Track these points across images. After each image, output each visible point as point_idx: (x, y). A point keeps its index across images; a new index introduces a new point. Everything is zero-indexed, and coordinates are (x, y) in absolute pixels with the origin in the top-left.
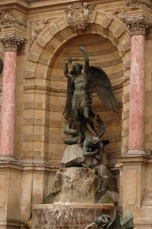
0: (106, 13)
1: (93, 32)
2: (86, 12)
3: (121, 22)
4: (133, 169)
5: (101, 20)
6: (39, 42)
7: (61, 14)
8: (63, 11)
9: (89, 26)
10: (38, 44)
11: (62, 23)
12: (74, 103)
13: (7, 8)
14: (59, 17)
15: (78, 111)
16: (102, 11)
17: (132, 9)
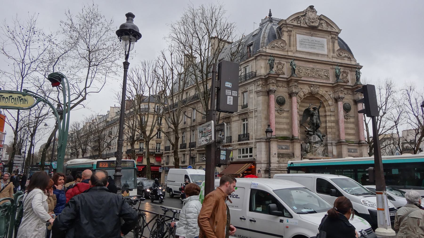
0: (323, 91)
1: (315, 96)
2: (318, 89)
3: (328, 95)
4: (345, 147)
5: (320, 93)
6: (299, 95)
7: (307, 87)
8: (308, 86)
9: (318, 93)
10: (299, 96)
11: (307, 90)
12: (315, 121)
13: (296, 81)
14: (306, 88)
15: (317, 123)
16: (321, 90)
17: (341, 93)
